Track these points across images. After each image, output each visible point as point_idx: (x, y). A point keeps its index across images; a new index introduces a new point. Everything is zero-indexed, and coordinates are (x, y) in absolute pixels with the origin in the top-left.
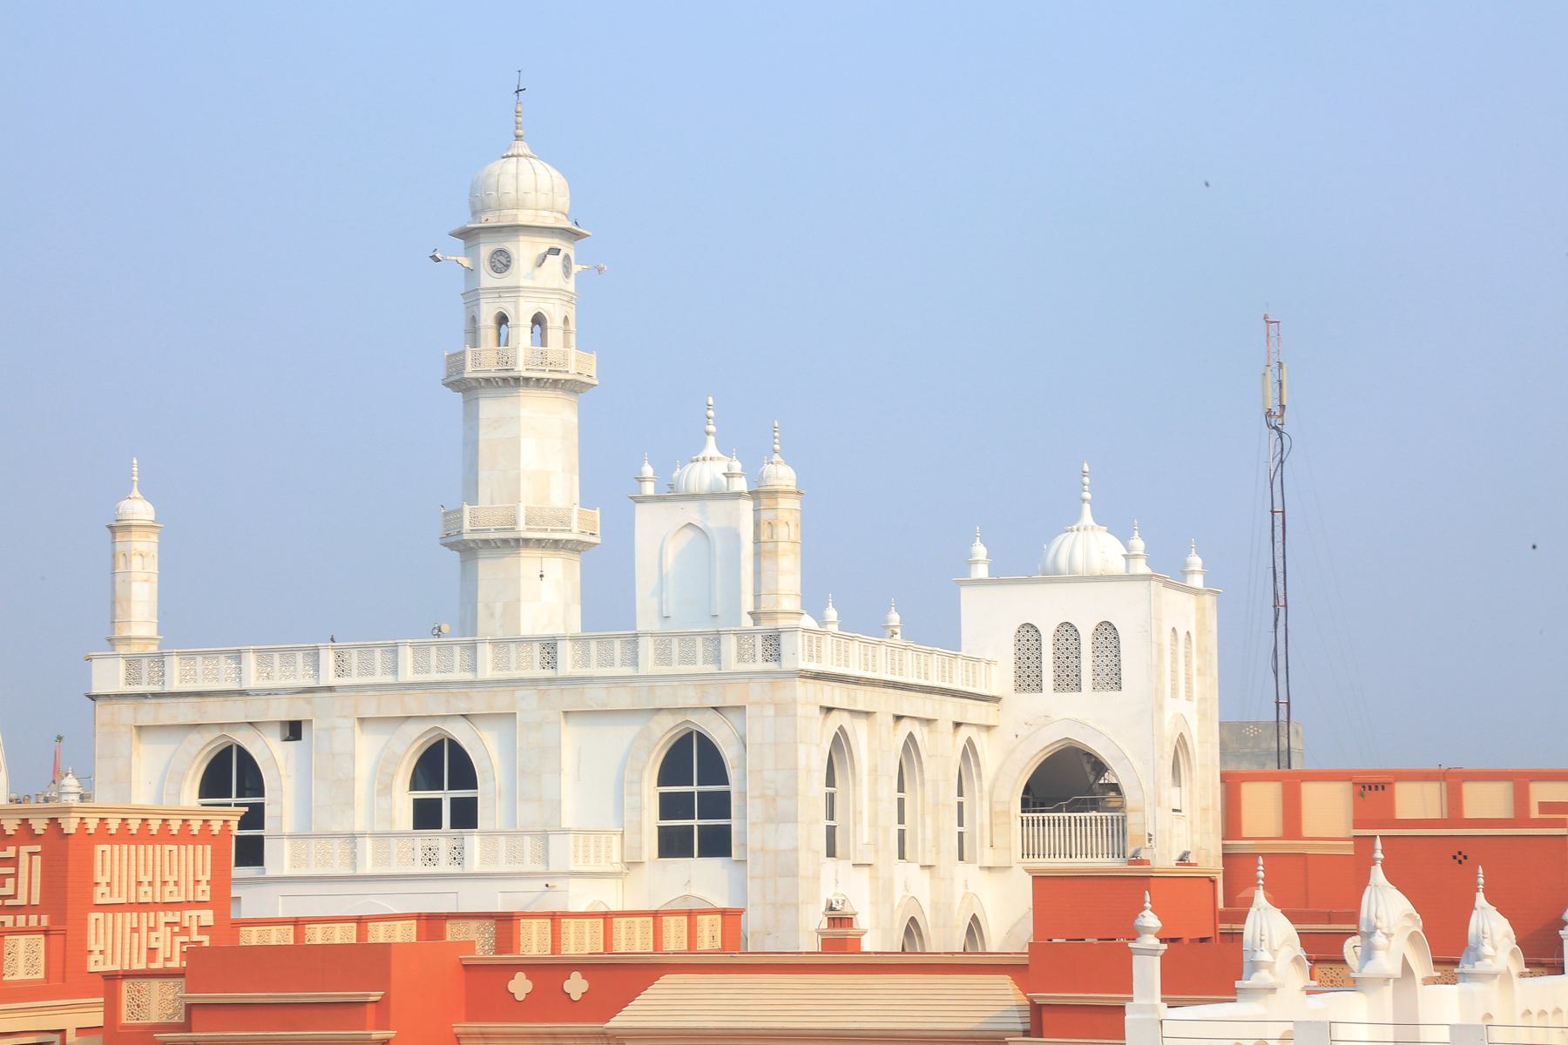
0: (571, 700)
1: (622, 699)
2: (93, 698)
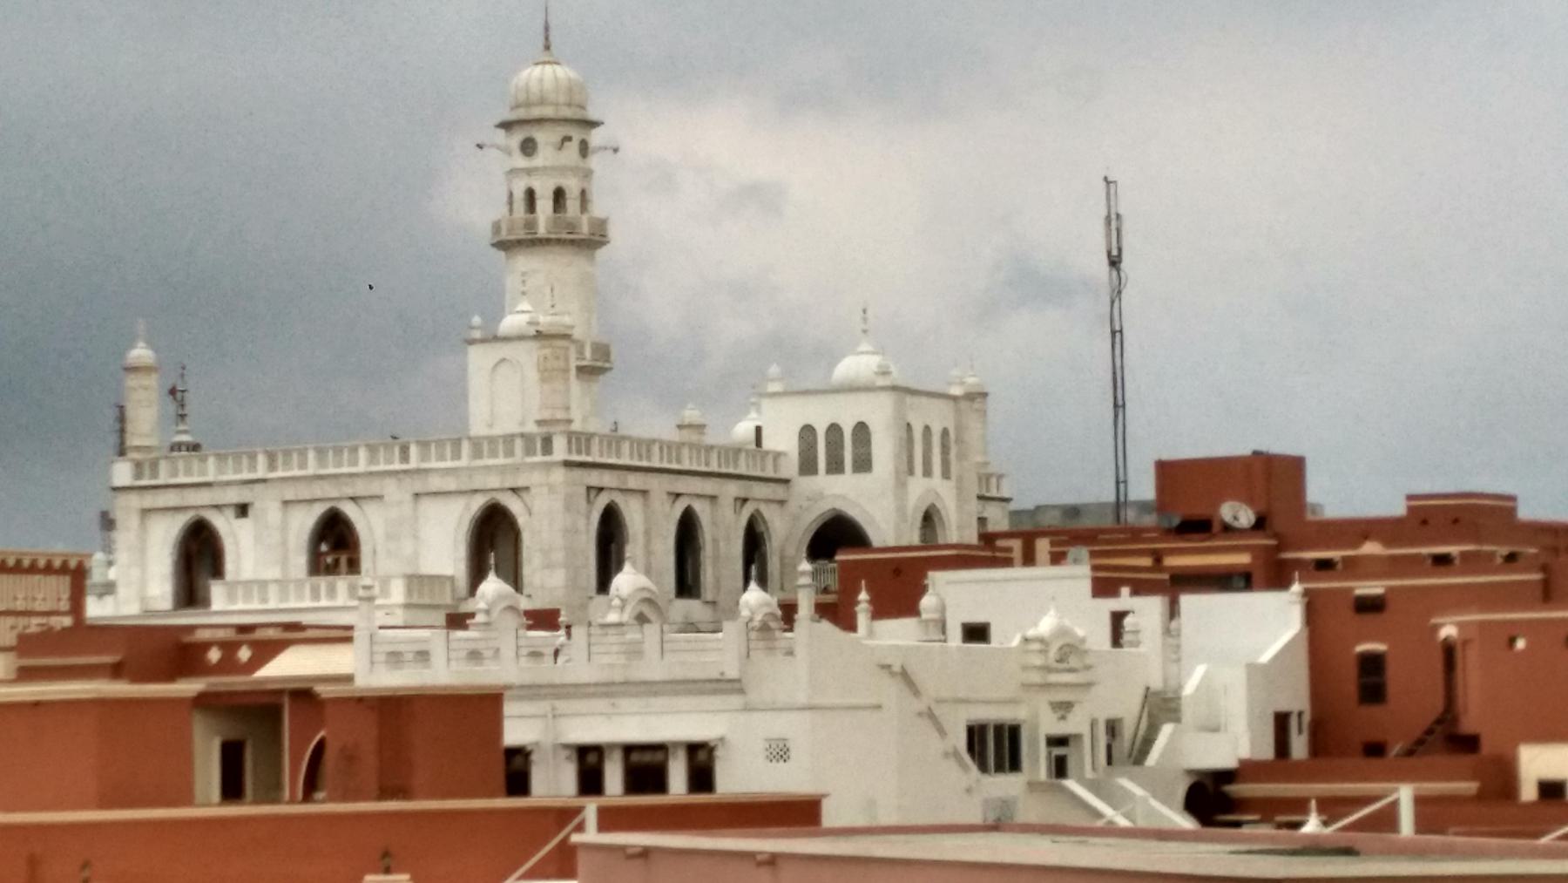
0: (418, 486)
1: (451, 484)
2: (116, 489)
